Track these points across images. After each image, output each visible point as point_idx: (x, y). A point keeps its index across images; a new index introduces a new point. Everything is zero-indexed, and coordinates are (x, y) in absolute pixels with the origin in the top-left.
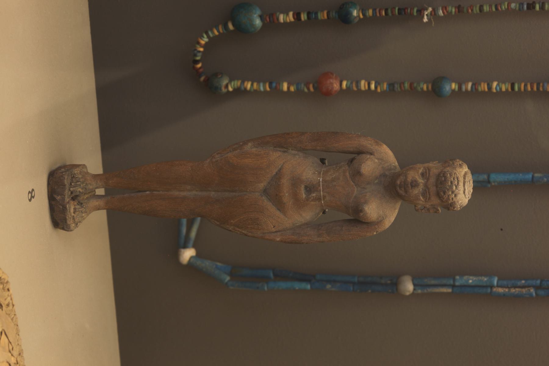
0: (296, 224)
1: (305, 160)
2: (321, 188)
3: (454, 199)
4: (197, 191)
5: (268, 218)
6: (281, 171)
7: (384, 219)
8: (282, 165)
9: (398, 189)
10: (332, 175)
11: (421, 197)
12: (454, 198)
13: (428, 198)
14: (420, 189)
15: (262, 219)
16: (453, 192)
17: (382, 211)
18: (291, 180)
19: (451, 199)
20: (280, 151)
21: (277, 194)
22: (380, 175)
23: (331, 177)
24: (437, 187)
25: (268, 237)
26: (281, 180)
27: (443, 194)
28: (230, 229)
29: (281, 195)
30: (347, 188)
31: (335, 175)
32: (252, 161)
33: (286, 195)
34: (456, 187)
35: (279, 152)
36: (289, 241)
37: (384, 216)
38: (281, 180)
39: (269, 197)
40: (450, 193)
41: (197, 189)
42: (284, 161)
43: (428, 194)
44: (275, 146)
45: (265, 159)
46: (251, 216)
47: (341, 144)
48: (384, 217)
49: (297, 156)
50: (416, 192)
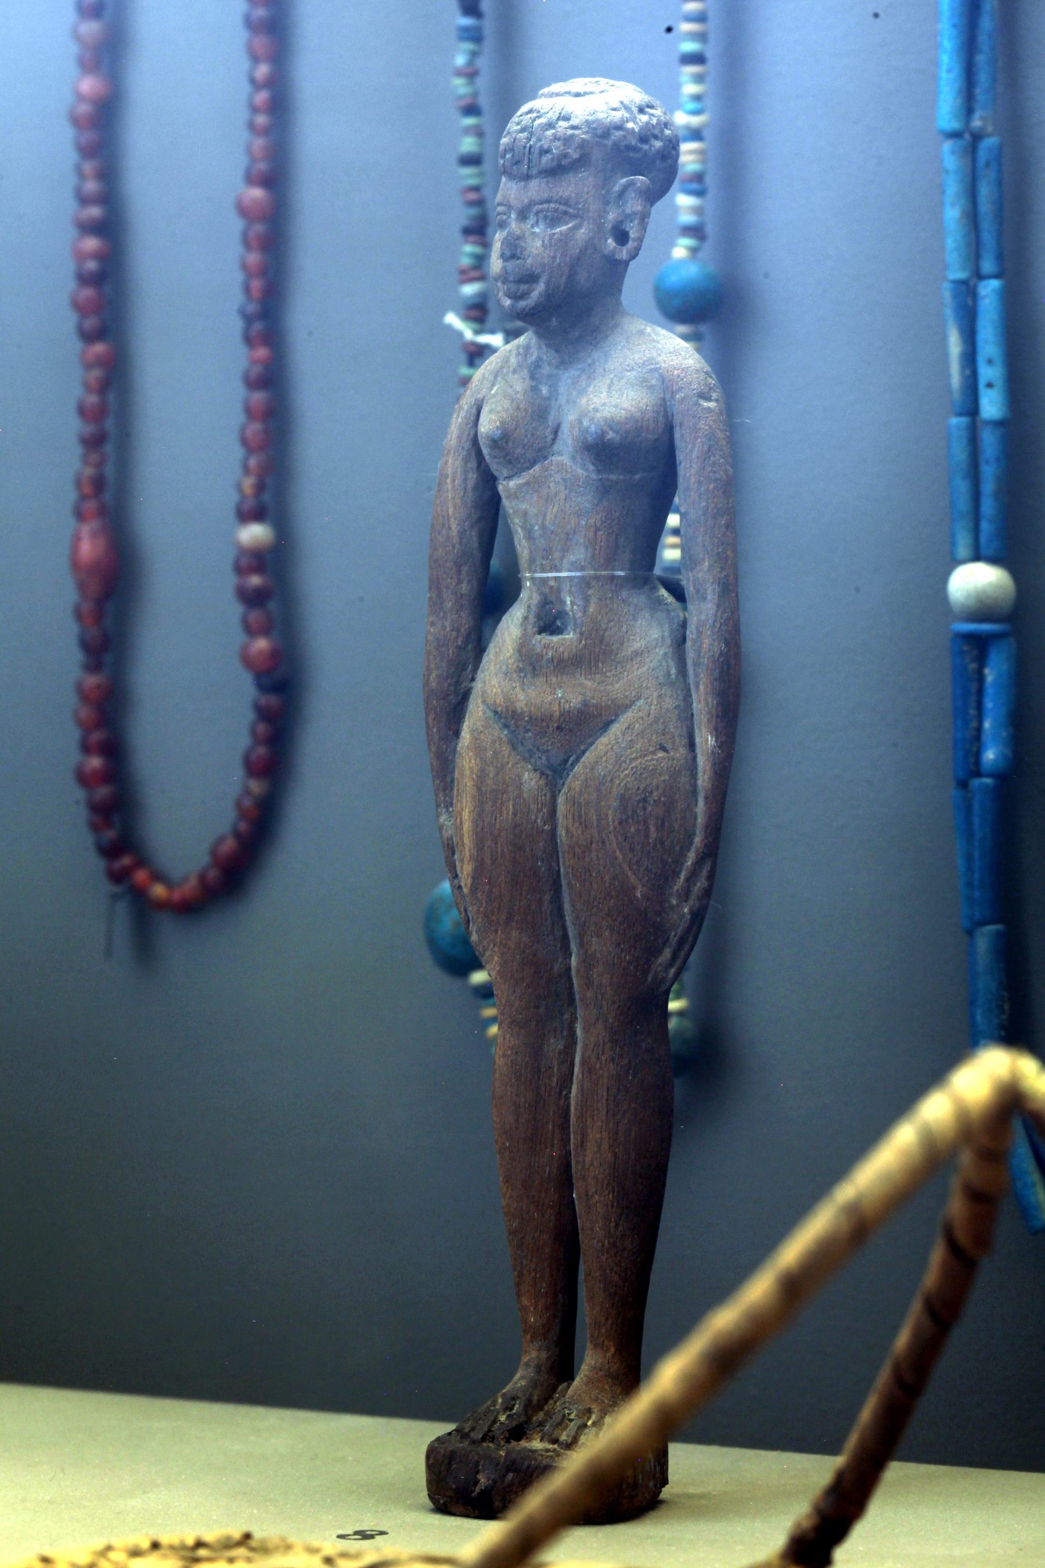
0: (669, 674)
2: (550, 575)
3: (574, 122)
4: (574, 1019)
5: (625, 762)
6: (499, 709)
7: (656, 370)
9: (522, 304)
11: (558, 229)
12: (572, 122)
13: (562, 208)
14: (534, 233)
15: (622, 784)
16: (550, 125)
17: (628, 374)
18: (524, 677)
19: (570, 132)
21: (555, 725)
22: (532, 377)
24: (527, 177)
25: (706, 777)
26: (519, 711)
27: (548, 155)
28: (686, 910)
29: (558, 713)
30: (549, 487)
33: (560, 695)
36: (715, 702)
37: (648, 367)
38: (519, 711)
39: (572, 759)
40: (550, 133)
41: (566, 1016)
43: (545, 206)
44: (451, 733)
46: (614, 822)
47: (451, 511)
48: (652, 367)
50: (539, 243)
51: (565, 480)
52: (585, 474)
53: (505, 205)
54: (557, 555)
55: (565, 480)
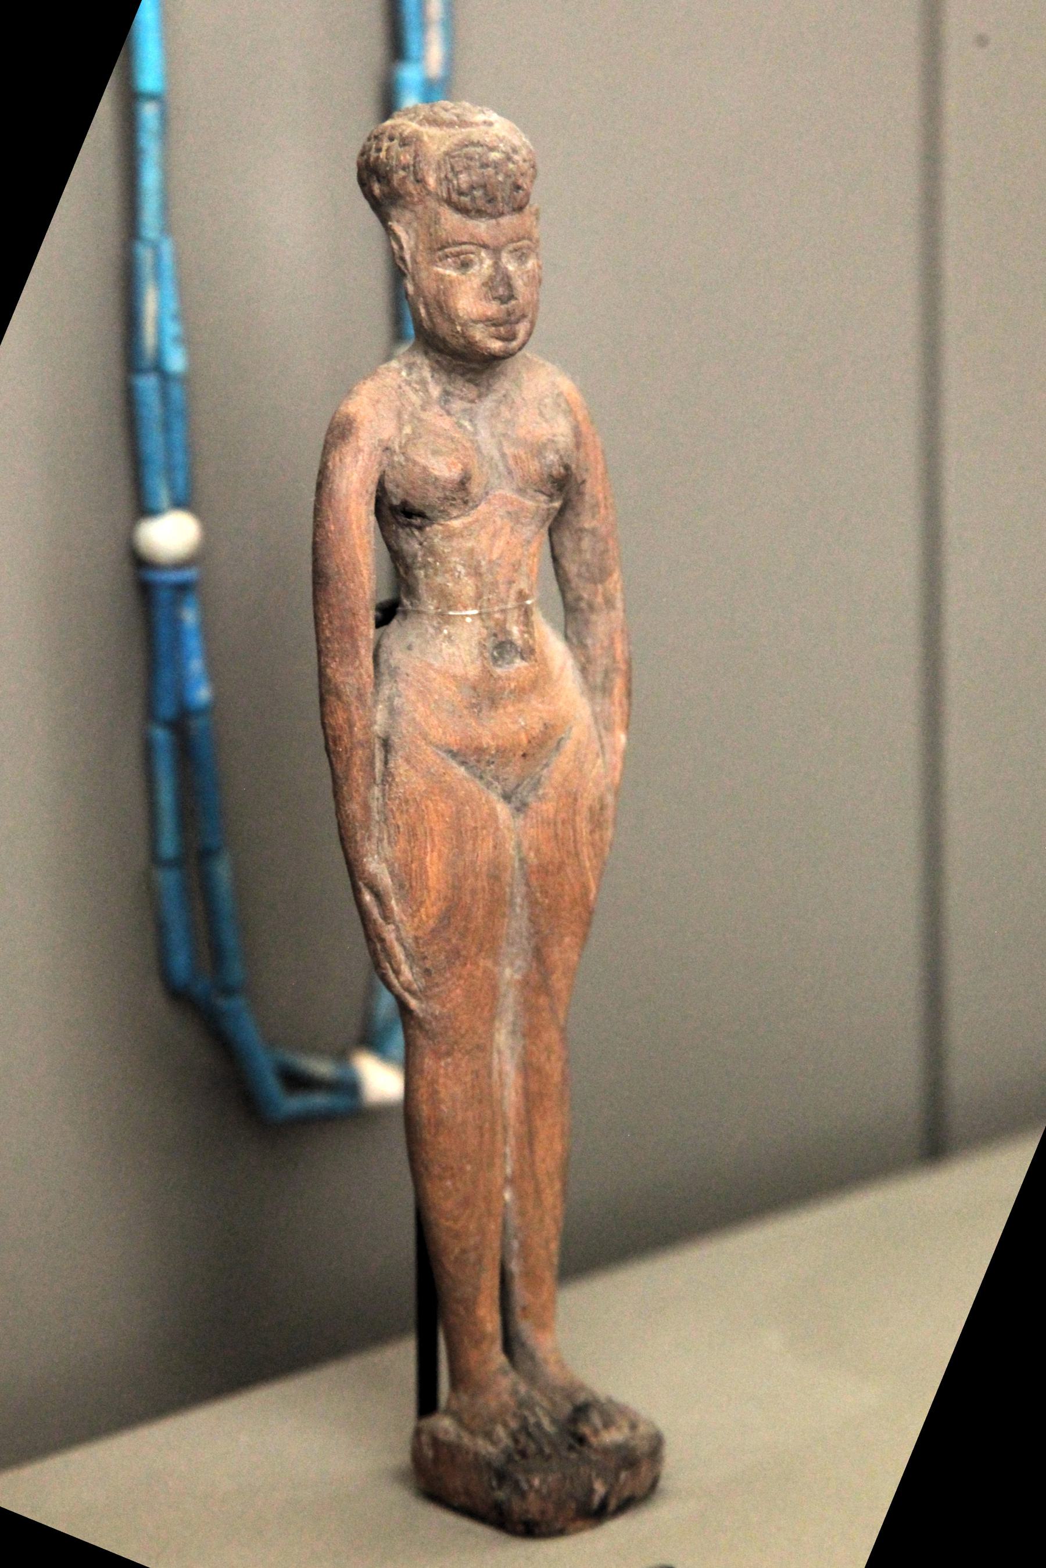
1: (408, 675)
6: (455, 749)
8: (437, 746)
10: (459, 577)
20: (386, 762)
21: (521, 753)
23: (466, 578)
30: (494, 522)
31: (460, 568)
32: (432, 851)
34: (492, 149)
35: (391, 765)
42: (423, 743)
43: (520, 244)
45: (424, 808)
49: (395, 703)
51: (509, 513)
52: (536, 505)
53: (476, 244)
54: (502, 588)
55: (509, 513)
